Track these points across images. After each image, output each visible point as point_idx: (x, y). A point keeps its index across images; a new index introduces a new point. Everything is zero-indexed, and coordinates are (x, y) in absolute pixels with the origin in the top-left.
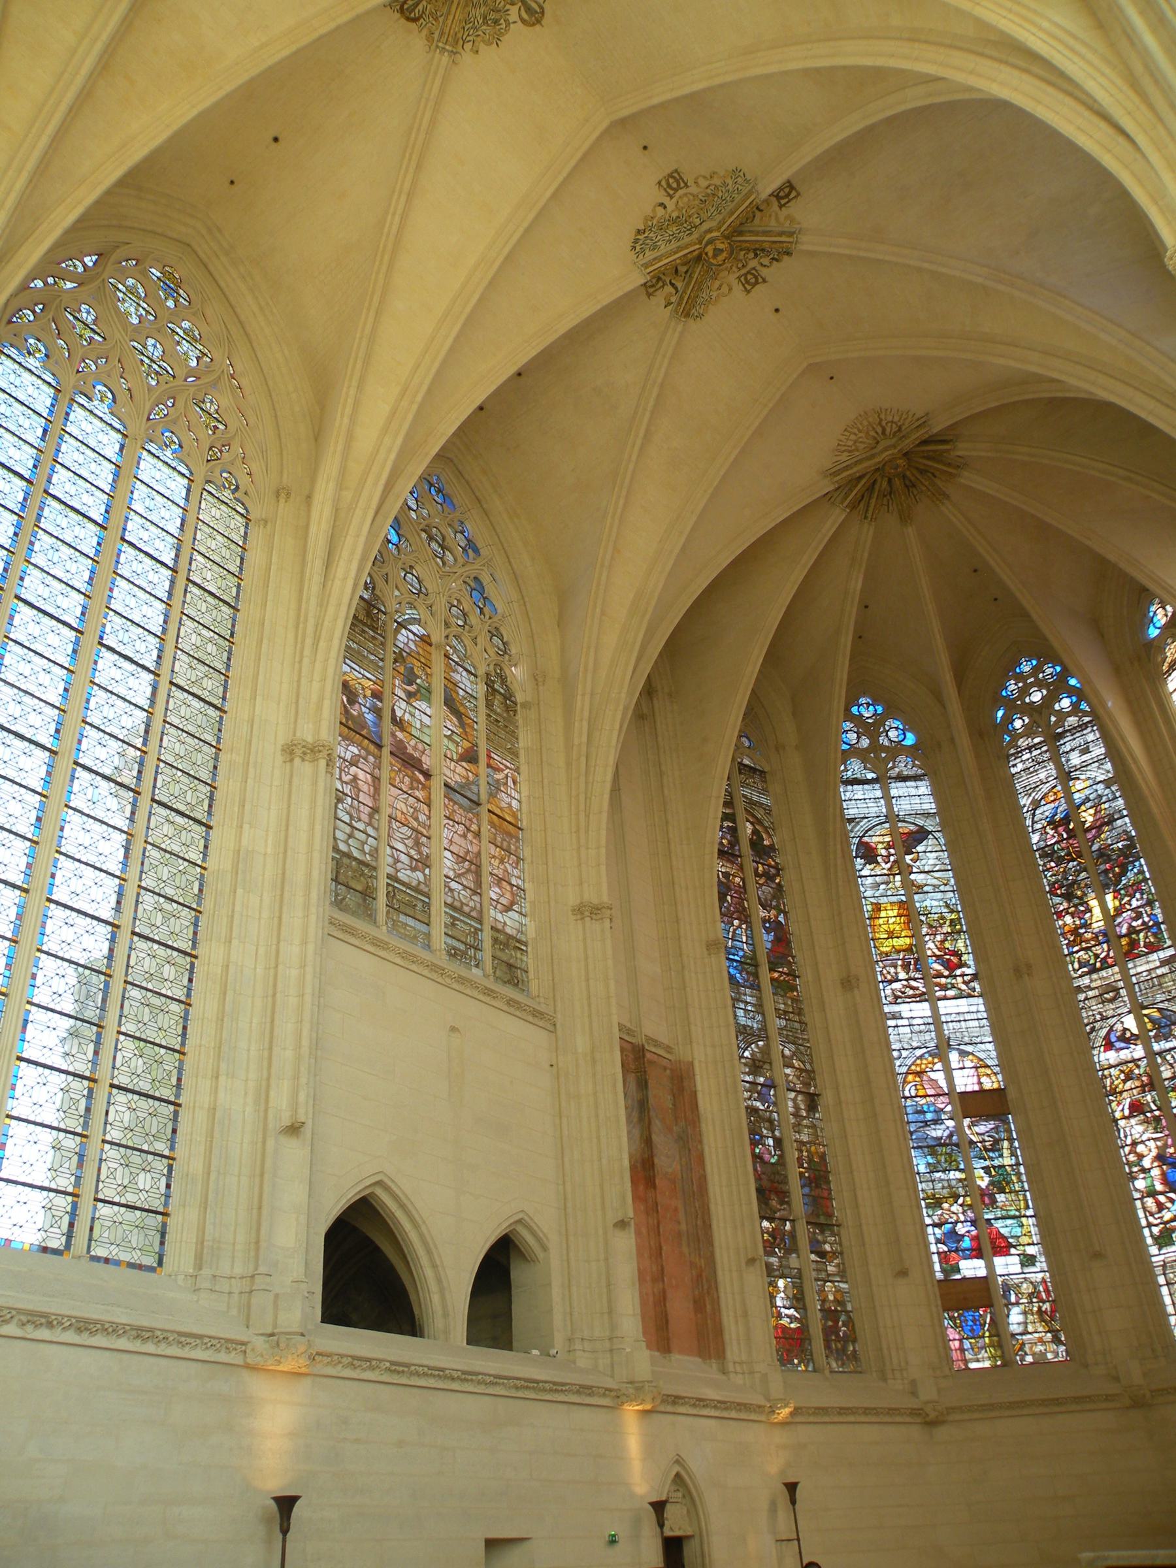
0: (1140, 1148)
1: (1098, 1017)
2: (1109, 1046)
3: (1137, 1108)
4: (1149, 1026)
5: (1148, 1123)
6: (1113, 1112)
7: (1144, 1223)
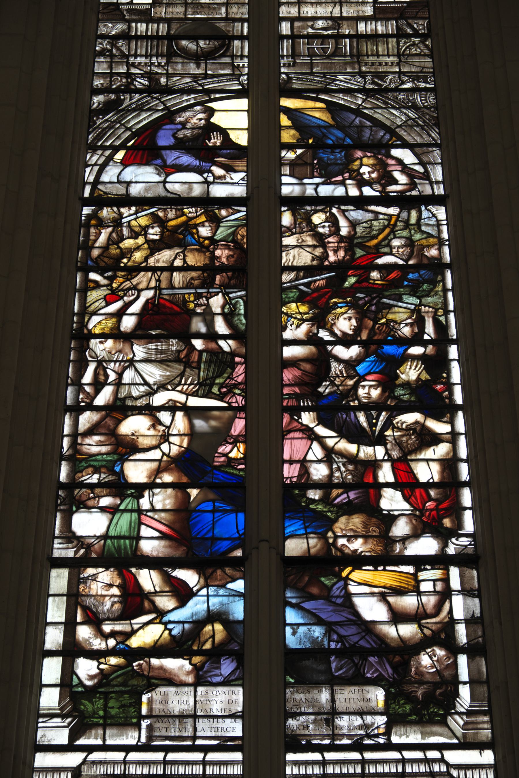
0: (134, 425)
1: (141, 83)
2: (144, 150)
3: (164, 320)
4: (288, 136)
5: (187, 364)
6: (86, 312)
7: (54, 637)
